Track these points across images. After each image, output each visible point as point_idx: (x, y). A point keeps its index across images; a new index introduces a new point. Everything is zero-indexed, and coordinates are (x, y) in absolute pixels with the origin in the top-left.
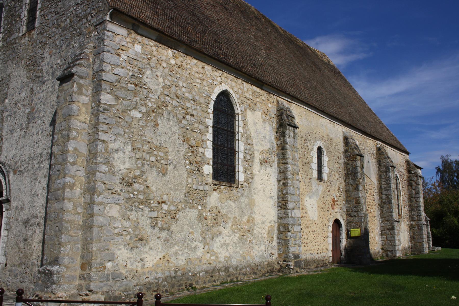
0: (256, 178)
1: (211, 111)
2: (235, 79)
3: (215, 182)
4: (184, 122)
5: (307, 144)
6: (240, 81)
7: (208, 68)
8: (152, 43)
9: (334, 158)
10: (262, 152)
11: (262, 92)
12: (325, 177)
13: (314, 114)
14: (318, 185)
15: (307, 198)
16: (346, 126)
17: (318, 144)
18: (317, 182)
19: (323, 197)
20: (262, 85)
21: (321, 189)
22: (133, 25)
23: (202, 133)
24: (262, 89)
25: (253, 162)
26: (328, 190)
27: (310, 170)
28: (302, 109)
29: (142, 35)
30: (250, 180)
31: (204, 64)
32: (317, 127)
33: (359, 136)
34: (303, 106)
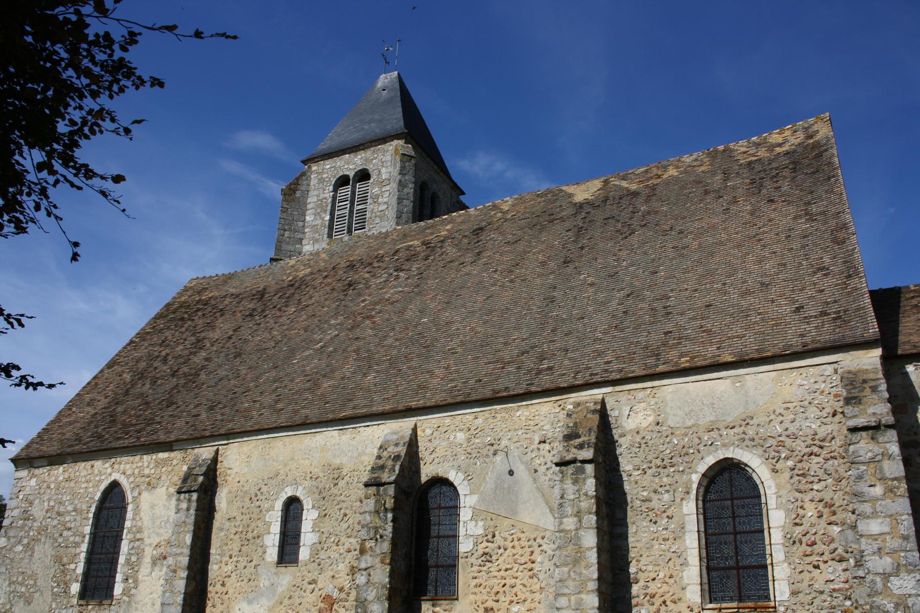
0: (141, 587)
1: (91, 515)
2: (131, 459)
3: (82, 602)
4: (60, 540)
5: (258, 503)
6: (138, 458)
7: (98, 464)
8: (45, 470)
9: (344, 505)
10: (158, 546)
11: (173, 454)
12: (304, 554)
13: (286, 439)
14: (276, 574)
15: (244, 605)
16: (405, 417)
17: (289, 492)
18: (273, 570)
19: (290, 598)
20: (172, 446)
21: (284, 582)
22: (30, 463)
23: (77, 545)
24: (172, 450)
25: (139, 565)
26: (307, 580)
27: (259, 549)
28: (254, 443)
29: (38, 467)
30: (133, 591)
31: (93, 462)
32: (293, 459)
33: (471, 417)
34: (254, 438)
